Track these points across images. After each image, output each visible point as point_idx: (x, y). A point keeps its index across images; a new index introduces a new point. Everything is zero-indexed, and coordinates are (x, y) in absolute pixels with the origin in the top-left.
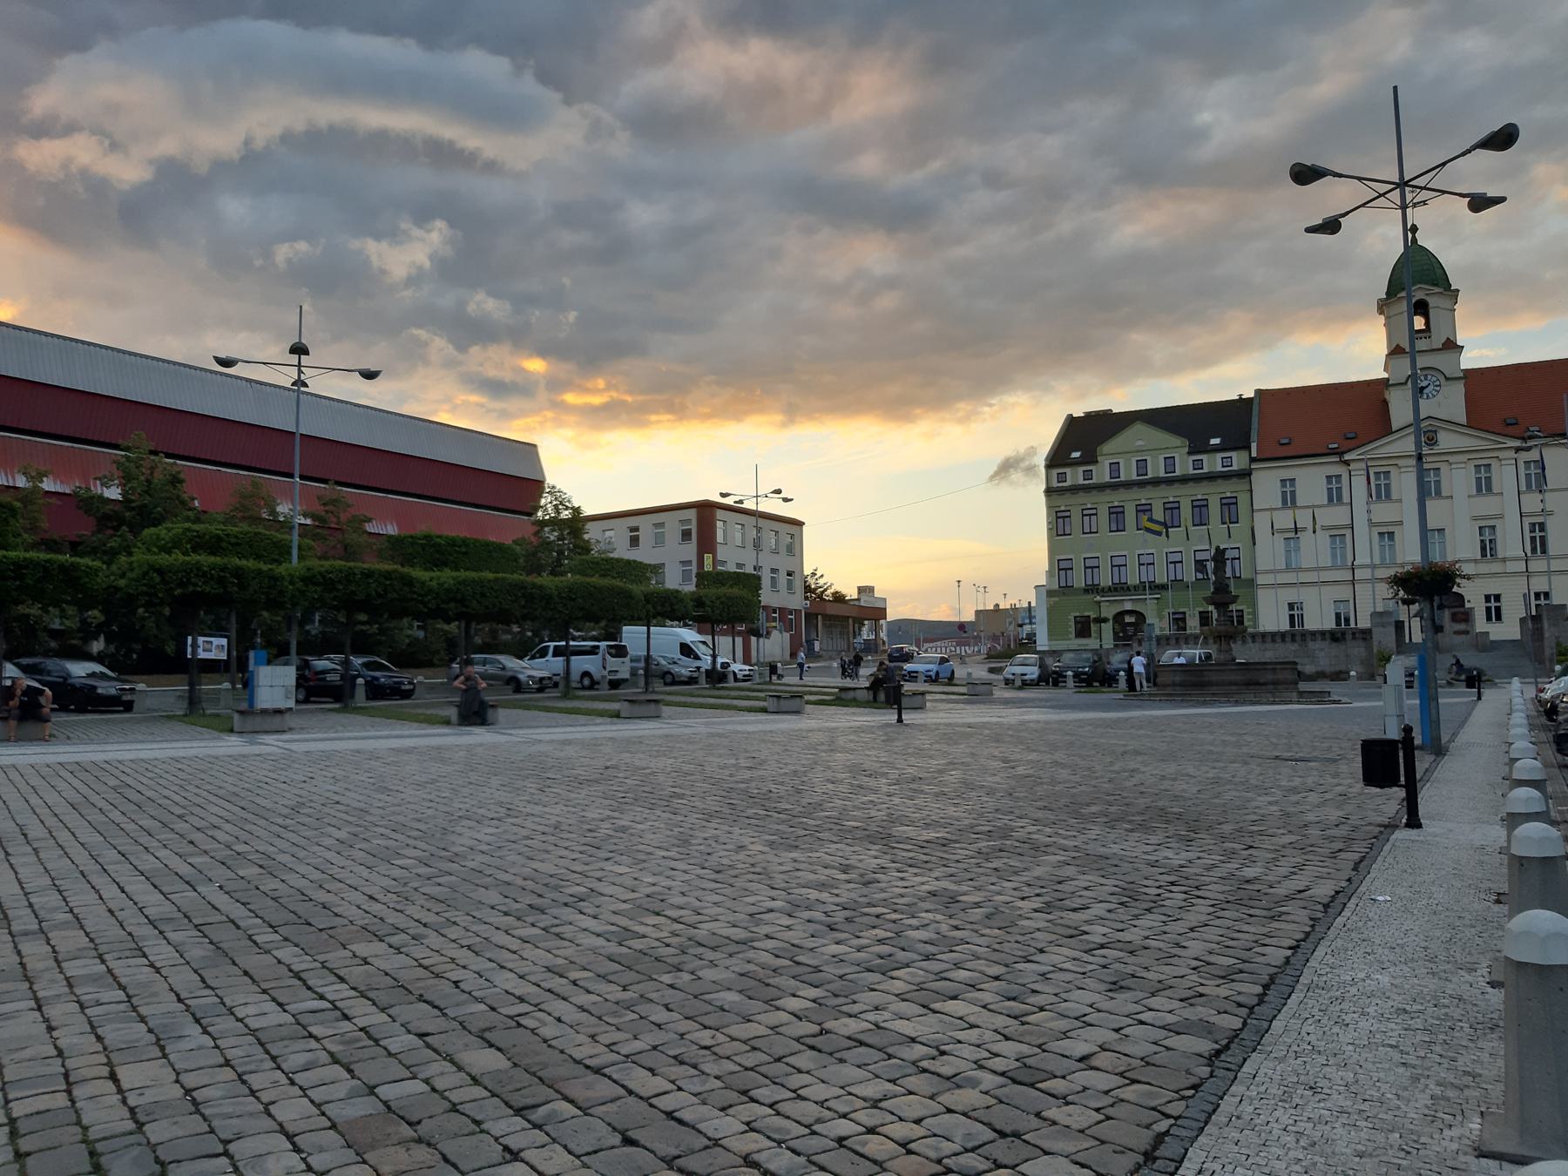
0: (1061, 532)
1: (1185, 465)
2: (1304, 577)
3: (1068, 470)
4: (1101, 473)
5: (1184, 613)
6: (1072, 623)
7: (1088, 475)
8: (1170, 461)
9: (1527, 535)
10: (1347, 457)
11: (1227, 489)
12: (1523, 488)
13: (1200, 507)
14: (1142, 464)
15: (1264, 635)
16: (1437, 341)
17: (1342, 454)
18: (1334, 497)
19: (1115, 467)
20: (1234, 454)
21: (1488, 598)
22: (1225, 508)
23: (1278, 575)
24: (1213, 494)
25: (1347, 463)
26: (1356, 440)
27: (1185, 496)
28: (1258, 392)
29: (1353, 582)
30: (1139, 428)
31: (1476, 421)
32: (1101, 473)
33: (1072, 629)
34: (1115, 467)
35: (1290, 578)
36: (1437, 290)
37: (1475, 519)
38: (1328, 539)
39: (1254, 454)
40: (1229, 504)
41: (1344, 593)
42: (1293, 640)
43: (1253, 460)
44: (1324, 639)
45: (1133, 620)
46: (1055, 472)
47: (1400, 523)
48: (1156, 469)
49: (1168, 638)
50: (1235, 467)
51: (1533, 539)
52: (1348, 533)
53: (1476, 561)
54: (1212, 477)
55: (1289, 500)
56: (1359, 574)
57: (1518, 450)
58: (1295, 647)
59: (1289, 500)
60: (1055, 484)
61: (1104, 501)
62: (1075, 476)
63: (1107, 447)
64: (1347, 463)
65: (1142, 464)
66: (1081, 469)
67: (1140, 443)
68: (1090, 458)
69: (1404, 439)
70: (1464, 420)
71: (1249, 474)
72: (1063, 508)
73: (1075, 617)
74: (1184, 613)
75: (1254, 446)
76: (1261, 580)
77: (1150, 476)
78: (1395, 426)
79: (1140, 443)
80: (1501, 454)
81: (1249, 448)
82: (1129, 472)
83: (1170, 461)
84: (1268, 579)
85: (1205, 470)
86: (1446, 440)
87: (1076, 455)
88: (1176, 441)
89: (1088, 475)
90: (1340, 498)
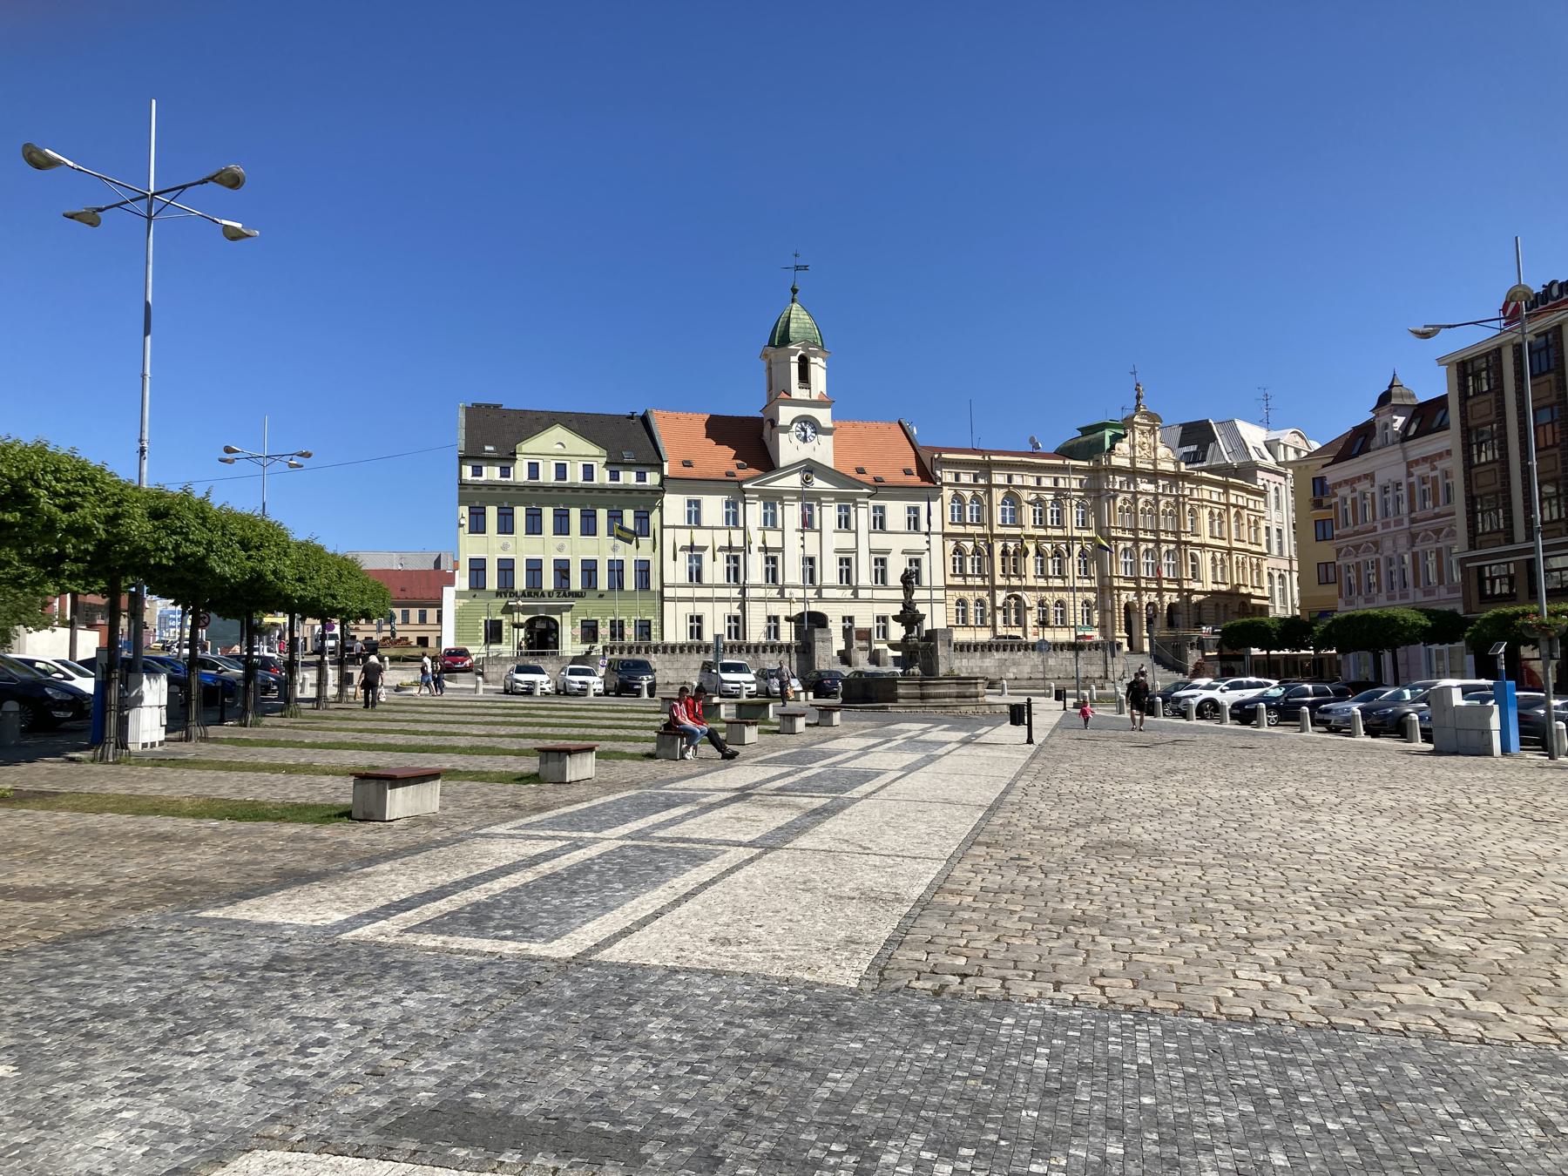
1: (602, 477)
4: (520, 474)
5: (596, 621)
6: (482, 628)
8: (588, 471)
9: (874, 567)
10: (745, 486)
14: (561, 470)
15: (673, 648)
18: (733, 519)
19: (534, 469)
21: (844, 619)
25: (744, 491)
30: (558, 433)
32: (520, 474)
33: (482, 634)
34: (534, 469)
37: (838, 551)
42: (665, 652)
44: (772, 652)
45: (544, 626)
48: (575, 476)
49: (682, 648)
52: (741, 555)
54: (628, 490)
55: (695, 518)
56: (751, 593)
57: (870, 496)
59: (695, 518)
62: (491, 473)
63: (527, 446)
65: (561, 470)
68: (512, 457)
71: (664, 491)
74: (596, 621)
75: (666, 465)
76: (668, 592)
77: (568, 481)
78: (782, 464)
81: (658, 466)
82: (547, 476)
83: (588, 471)
85: (621, 482)
88: (594, 450)
90: (736, 522)
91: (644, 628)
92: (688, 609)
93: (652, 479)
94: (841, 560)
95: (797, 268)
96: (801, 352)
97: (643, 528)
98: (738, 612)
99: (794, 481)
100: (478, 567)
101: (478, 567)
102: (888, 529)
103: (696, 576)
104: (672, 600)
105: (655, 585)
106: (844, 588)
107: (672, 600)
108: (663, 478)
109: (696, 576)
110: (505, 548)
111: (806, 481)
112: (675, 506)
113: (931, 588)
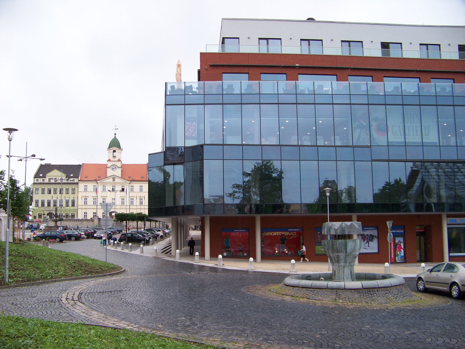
0: (36, 193)
2: (87, 207)
3: (39, 179)
4: (46, 180)
7: (43, 180)
10: (97, 182)
11: (73, 186)
12: (130, 191)
13: (67, 190)
16: (117, 159)
17: (97, 181)
20: (75, 179)
22: (73, 191)
23: (83, 206)
24: (70, 187)
25: (98, 183)
26: (100, 178)
27: (64, 187)
28: (83, 164)
29: (97, 209)
31: (122, 177)
32: (46, 180)
35: (84, 207)
36: (118, 148)
37: (121, 197)
38: (93, 199)
39: (79, 179)
40: (73, 190)
41: (95, 211)
43: (79, 181)
46: (36, 179)
47: (107, 197)
50: (75, 182)
51: (131, 201)
53: (120, 206)
55: (86, 190)
57: (130, 183)
58: (80, 222)
59: (86, 190)
60: (36, 182)
61: (46, 187)
62: (40, 180)
64: (98, 183)
66: (42, 179)
67: (55, 174)
69: (109, 179)
70: (120, 176)
72: (37, 188)
73: (39, 214)
75: (79, 177)
76: (79, 207)
78: (108, 176)
79: (55, 174)
80: (127, 184)
81: (78, 178)
82: (53, 181)
84: (80, 207)
86: (117, 180)
87: (41, 175)
88: (63, 175)
89: (43, 180)
91: (73, 216)
92: (84, 211)
93: (76, 180)
94: (122, 199)
95: (116, 129)
96: (114, 149)
97: (74, 192)
98: (95, 211)
99: (111, 180)
100: (37, 202)
101: (37, 202)
102: (134, 191)
103: (86, 203)
104: (80, 208)
105: (76, 205)
106: (123, 206)
107: (80, 208)
108: (79, 181)
109: (86, 203)
110: (43, 197)
111: (114, 180)
112: (81, 186)
113: (144, 206)
